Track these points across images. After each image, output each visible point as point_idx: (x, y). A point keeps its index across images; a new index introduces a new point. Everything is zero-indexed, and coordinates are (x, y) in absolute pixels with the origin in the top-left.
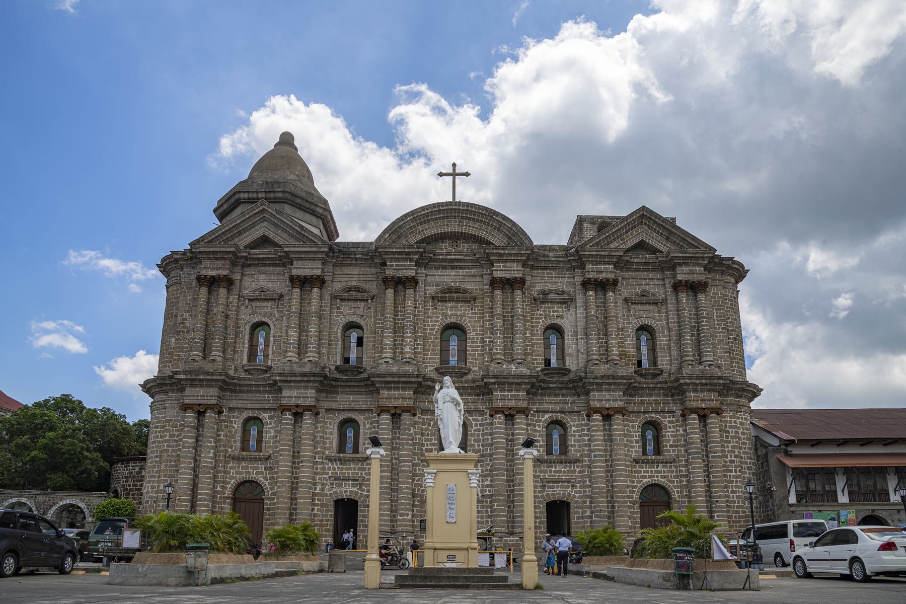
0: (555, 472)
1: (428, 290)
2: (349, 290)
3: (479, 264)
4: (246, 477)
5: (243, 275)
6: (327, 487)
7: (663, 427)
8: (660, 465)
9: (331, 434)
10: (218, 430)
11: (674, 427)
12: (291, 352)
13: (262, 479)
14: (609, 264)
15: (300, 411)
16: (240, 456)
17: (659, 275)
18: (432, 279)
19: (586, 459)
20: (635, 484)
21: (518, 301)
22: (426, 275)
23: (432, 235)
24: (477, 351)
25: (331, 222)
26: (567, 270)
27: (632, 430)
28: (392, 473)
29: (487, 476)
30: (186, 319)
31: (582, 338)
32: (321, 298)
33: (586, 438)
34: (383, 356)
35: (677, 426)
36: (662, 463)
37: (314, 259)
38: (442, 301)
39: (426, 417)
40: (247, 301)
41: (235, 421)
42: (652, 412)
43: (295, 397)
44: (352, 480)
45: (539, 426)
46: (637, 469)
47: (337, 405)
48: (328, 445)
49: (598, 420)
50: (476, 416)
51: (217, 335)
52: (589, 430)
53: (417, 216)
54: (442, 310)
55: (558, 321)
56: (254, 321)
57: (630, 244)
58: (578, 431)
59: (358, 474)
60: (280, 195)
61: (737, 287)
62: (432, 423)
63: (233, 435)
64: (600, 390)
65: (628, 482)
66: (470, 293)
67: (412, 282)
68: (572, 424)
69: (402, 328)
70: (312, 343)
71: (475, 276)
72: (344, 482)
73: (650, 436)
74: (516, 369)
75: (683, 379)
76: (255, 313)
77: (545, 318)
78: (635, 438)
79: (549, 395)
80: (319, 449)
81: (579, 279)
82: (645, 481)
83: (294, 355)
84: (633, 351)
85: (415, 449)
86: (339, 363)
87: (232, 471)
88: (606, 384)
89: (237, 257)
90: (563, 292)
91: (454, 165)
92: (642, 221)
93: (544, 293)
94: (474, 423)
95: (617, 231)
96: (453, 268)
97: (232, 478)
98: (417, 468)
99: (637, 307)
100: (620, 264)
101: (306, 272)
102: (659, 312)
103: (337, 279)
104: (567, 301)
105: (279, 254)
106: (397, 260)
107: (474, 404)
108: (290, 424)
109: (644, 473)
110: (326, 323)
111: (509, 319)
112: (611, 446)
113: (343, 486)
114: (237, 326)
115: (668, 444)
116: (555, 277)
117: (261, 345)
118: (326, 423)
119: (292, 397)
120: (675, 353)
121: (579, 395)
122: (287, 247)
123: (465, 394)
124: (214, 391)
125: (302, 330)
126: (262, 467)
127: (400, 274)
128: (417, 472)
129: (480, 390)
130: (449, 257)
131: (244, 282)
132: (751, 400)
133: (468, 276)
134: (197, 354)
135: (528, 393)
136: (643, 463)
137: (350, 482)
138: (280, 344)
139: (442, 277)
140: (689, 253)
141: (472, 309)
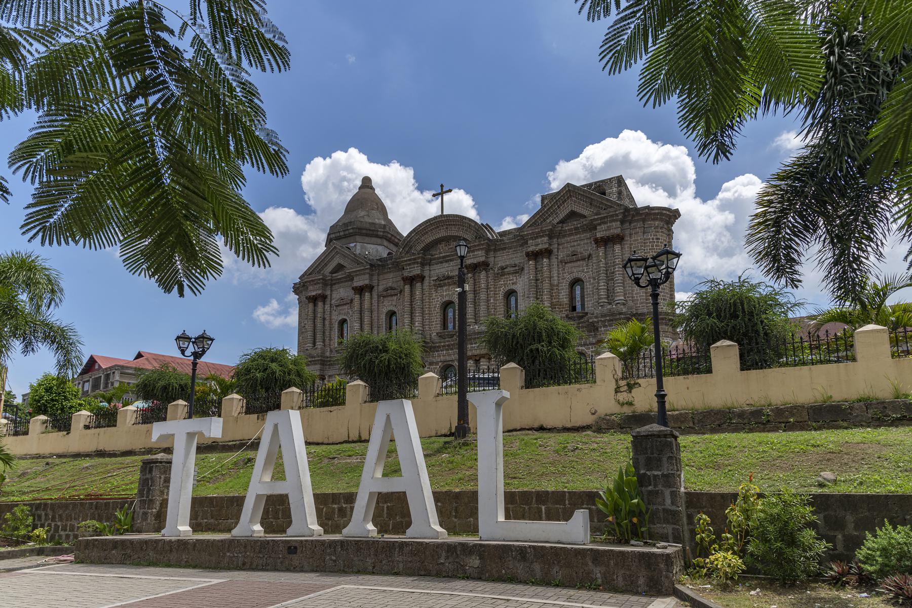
2: (386, 290)
5: (331, 291)
37: (364, 274)
38: (441, 287)
55: (514, 287)
57: (561, 216)
60: (351, 231)
76: (340, 314)
84: (565, 300)
89: (326, 281)
90: (515, 266)
91: (442, 186)
93: (503, 268)
99: (570, 265)
106: (409, 265)
110: (375, 314)
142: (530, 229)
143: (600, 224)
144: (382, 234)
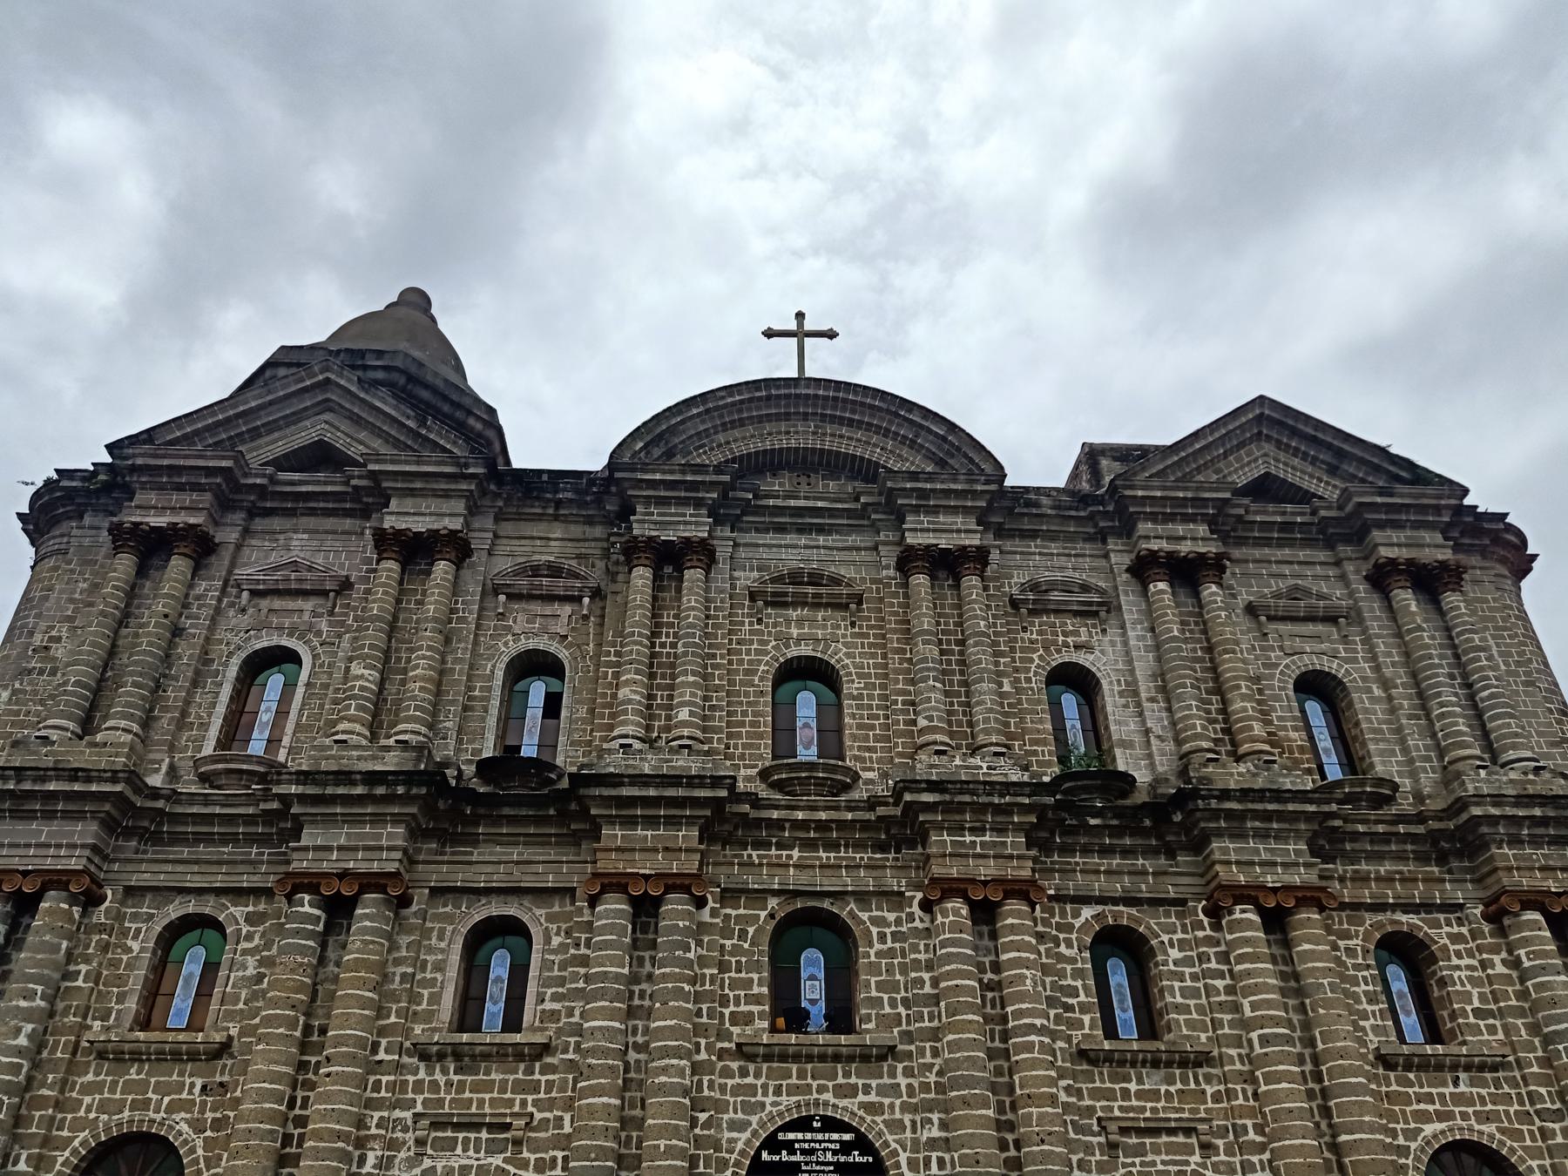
0: (1140, 1095)
1: (738, 579)
3: (866, 522)
4: (131, 1122)
5: (246, 532)
6: (402, 1155)
7: (1438, 954)
8: (1462, 1076)
9: (440, 967)
10: (70, 957)
11: (1470, 954)
12: (350, 721)
13: (184, 1127)
14: (1194, 521)
16: (127, 1047)
17: (1322, 555)
18: (750, 555)
19: (1233, 1052)
20: (1401, 1141)
21: (975, 601)
23: (749, 454)
24: (873, 727)
26: (1085, 540)
27: (1350, 962)
28: (623, 1099)
29: (929, 1107)
30: (58, 639)
31: (1152, 700)
32: (456, 588)
33: (1219, 983)
34: (614, 734)
35: (1480, 949)
36: (1467, 1068)
37: (446, 495)
38: (774, 604)
39: (734, 913)
40: (245, 595)
41: (138, 931)
42: (1394, 907)
43: (340, 848)
44: (492, 1127)
45: (1069, 945)
46: (1394, 1087)
47: (469, 876)
48: (424, 1006)
49: (1249, 925)
50: (880, 908)
51: (132, 674)
52: (1224, 957)
53: (717, 408)
54: (775, 625)
55: (1082, 659)
56: (258, 647)
57: (1241, 479)
58: (1187, 961)
59: (511, 1102)
62: (751, 930)
63: (119, 977)
64: (1240, 835)
66: (848, 585)
67: (704, 553)
68: (1165, 938)
69: (673, 666)
70: (414, 698)
71: (858, 549)
72: (461, 1136)
74: (989, 768)
75: (1477, 804)
77: (1046, 649)
78: (1364, 987)
79: (1086, 851)
80: (393, 1019)
81: (1121, 560)
82: (1429, 1129)
83: (358, 727)
85: (699, 1013)
86: (488, 753)
87: (87, 1100)
88: (1258, 816)
89: (238, 488)
90: (1085, 588)
92: (1260, 433)
94: (874, 930)
96: (802, 530)
97: (77, 1126)
98: (706, 1079)
100: (1225, 524)
101: (420, 525)
102: (1345, 639)
103: (504, 547)
104: (1100, 610)
105: (354, 482)
106: (662, 502)
107: (875, 873)
108: (311, 935)
109: (1419, 1101)
110: (462, 650)
111: (954, 646)
112: (1302, 1009)
113: (459, 1151)
114: (205, 659)
115: (1469, 1008)
116: (1058, 555)
117: (268, 710)
118: (425, 934)
119: (329, 849)
120: (1417, 742)
121: (1171, 854)
122: (377, 462)
123: (847, 846)
124: (86, 831)
125: (389, 664)
126: (192, 1085)
127: (669, 535)
128: (706, 1093)
129: (887, 833)
130: (792, 503)
131: (246, 551)
133: (838, 549)
134: (60, 727)
136: (1408, 1067)
137: (484, 1135)
138: (322, 706)
139: (774, 550)
140: (1402, 496)
141: (853, 624)
142: (1156, 482)
143: (1381, 525)
144: (479, 426)
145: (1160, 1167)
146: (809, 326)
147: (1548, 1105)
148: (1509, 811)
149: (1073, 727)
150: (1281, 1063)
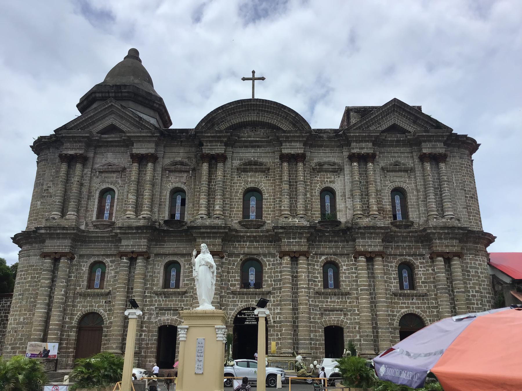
0: (330, 302)
1: (234, 163)
2: (175, 163)
3: (271, 144)
4: (90, 310)
5: (95, 153)
6: (153, 316)
7: (416, 267)
8: (415, 298)
9: (159, 273)
10: (70, 273)
11: (424, 267)
12: (130, 211)
13: (102, 311)
14: (368, 142)
15: (134, 256)
16: (86, 293)
17: (408, 150)
18: (237, 155)
19: (355, 292)
20: (395, 313)
21: (300, 171)
22: (233, 152)
23: (237, 123)
24: (270, 208)
25: (165, 114)
26: (337, 147)
27: (391, 269)
29: (278, 305)
30: (50, 187)
31: (349, 198)
32: (154, 170)
33: (354, 275)
34: (199, 213)
35: (427, 266)
36: (416, 296)
38: (244, 171)
39: (231, 259)
40: (97, 172)
41: (84, 265)
42: (406, 255)
43: (131, 245)
44: (173, 310)
45: (317, 266)
46: (396, 301)
47: (164, 251)
48: (156, 282)
49: (362, 261)
50: (269, 257)
51: (72, 199)
52: (356, 269)
53: (226, 110)
54: (244, 178)
55: (332, 186)
56: (103, 188)
57: (384, 127)
58: (348, 269)
59: (178, 305)
60: (126, 94)
61: (471, 157)
63: (81, 276)
64: (364, 238)
65: (389, 311)
66: (265, 165)
67: (223, 158)
68: (343, 264)
69: (214, 191)
70: (146, 204)
71: (269, 153)
72: (167, 312)
73: (405, 274)
74: (298, 221)
75: (430, 229)
76: (103, 182)
77: (321, 183)
78: (393, 276)
79: (325, 242)
80: (148, 286)
81: (346, 154)
82: (403, 310)
83: (132, 213)
84: (389, 207)
85: (222, 284)
86: (166, 218)
87: (79, 305)
88: (368, 233)
90: (334, 164)
91: (253, 72)
92: (394, 110)
93: (320, 164)
94: (267, 263)
95: (374, 117)
96: (253, 147)
97: (78, 311)
98: (224, 299)
99: (391, 174)
100: (378, 142)
101: (143, 151)
102: (409, 177)
103: (168, 155)
104: (338, 170)
105: (123, 138)
106: (210, 142)
107: (268, 249)
108: (127, 266)
110: (158, 188)
111: (292, 184)
112: (374, 282)
113: (166, 315)
115: (420, 281)
116: (328, 152)
117: (108, 205)
118: (154, 265)
119: (129, 246)
120: (422, 209)
121: (348, 242)
122: (129, 133)
123: (261, 241)
124: (67, 242)
125: (139, 194)
126: (103, 302)
127: (213, 152)
128: (224, 302)
129: (272, 238)
130: (249, 139)
131: (96, 159)
132: (488, 245)
133: (263, 153)
134: (56, 214)
135: (308, 240)
136: (400, 296)
137: (172, 312)
138: (122, 205)
139: (244, 153)
140: (432, 132)
141: (266, 177)
142: (357, 131)
145: (333, 319)
146: (256, 76)
147: (435, 305)
148: (438, 231)
149: (328, 205)
150: (364, 296)
